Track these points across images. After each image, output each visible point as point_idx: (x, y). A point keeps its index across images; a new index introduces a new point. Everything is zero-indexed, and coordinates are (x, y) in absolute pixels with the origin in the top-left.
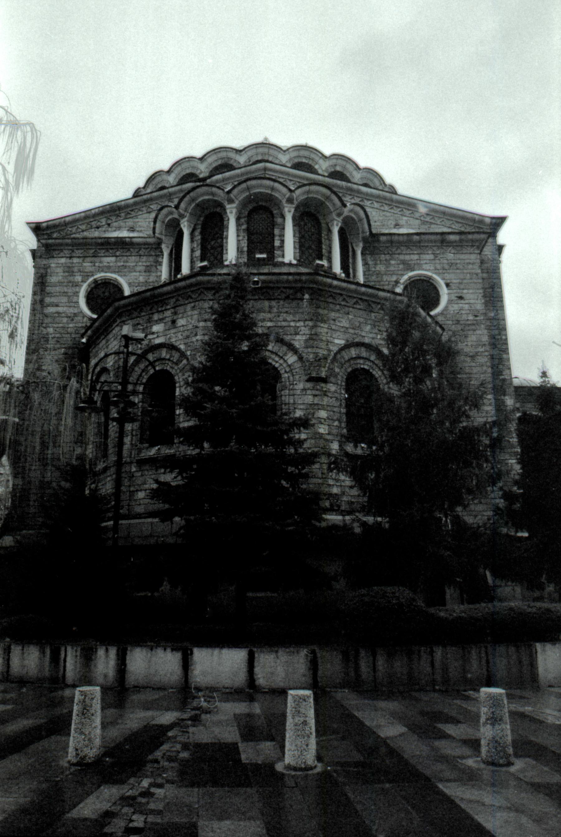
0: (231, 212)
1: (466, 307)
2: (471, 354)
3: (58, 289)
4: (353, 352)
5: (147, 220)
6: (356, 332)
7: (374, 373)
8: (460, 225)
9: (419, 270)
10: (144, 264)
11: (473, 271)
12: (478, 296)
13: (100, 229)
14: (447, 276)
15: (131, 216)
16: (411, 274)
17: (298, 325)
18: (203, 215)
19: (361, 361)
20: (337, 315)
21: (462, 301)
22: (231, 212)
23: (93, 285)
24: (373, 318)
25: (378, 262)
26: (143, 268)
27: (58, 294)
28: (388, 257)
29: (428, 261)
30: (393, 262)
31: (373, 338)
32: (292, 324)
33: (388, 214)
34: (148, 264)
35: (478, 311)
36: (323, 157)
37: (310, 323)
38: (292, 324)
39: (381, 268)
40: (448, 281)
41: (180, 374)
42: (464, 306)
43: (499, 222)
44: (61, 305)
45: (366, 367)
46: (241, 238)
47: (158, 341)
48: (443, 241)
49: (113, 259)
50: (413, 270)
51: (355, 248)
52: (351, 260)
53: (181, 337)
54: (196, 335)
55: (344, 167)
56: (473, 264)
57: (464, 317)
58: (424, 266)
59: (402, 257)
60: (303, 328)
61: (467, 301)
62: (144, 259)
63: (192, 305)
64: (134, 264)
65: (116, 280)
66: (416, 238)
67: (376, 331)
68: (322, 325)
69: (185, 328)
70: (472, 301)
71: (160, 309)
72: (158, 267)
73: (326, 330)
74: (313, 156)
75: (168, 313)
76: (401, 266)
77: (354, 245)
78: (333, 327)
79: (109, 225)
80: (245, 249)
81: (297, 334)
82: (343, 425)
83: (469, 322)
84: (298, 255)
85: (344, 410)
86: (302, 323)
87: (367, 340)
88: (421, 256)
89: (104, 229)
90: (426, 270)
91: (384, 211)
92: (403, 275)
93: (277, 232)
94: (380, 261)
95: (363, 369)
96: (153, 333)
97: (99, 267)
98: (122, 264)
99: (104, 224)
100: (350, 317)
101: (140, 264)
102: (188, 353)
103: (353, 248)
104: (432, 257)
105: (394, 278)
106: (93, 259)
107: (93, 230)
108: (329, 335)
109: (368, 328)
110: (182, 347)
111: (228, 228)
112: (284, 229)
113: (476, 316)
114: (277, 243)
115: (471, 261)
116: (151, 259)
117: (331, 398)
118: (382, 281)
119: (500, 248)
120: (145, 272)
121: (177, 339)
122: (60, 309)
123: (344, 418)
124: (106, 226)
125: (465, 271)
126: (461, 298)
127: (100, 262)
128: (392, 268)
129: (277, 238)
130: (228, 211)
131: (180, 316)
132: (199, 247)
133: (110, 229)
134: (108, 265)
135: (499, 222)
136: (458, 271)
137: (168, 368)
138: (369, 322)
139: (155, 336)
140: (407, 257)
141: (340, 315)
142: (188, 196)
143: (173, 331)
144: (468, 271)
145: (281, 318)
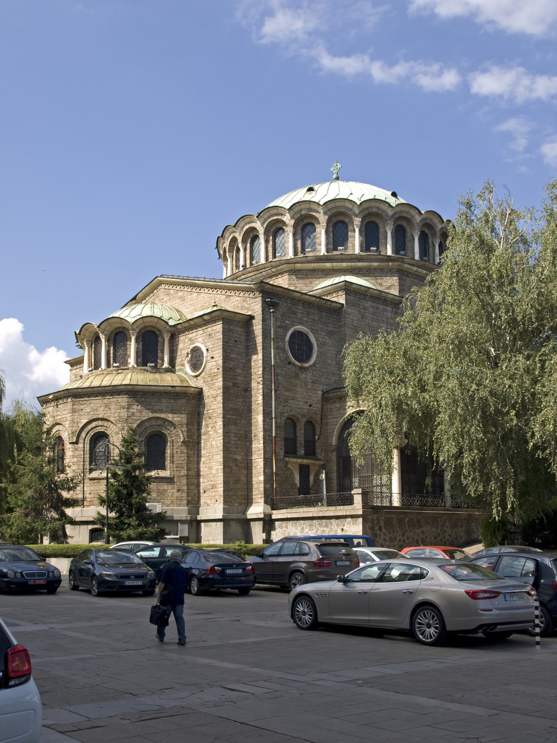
4: (94, 424)
6: (95, 412)
19: (100, 428)
20: (84, 406)
29: (200, 336)
30: (186, 340)
31: (105, 414)
32: (65, 416)
67: (107, 409)
73: (77, 416)
74: (280, 212)
78: (81, 414)
87: (100, 416)
95: (101, 431)
100: (91, 405)
108: (79, 418)
141: (86, 406)
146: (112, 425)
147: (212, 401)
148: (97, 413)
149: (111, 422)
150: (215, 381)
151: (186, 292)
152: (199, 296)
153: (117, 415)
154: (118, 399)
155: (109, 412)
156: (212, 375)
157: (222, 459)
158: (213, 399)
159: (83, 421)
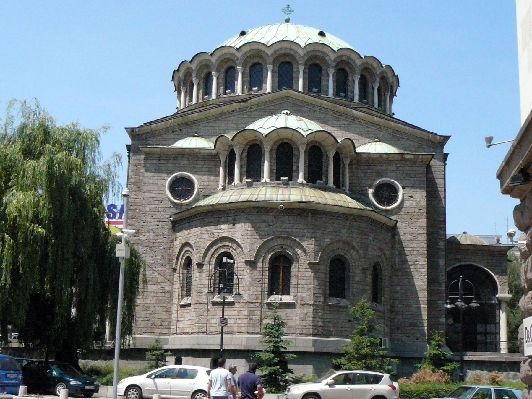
0: (267, 148)
1: (415, 203)
2: (415, 235)
3: (151, 181)
5: (207, 128)
7: (347, 257)
8: (419, 139)
9: (386, 177)
10: (208, 166)
11: (421, 179)
12: (423, 196)
13: (175, 133)
14: (404, 182)
15: (196, 124)
16: (379, 180)
17: (304, 231)
18: (249, 144)
21: (412, 199)
22: (267, 148)
23: (174, 179)
24: (348, 224)
25: (360, 171)
26: (207, 169)
27: (152, 185)
28: (366, 167)
30: (369, 171)
32: (302, 231)
33: (370, 130)
34: (210, 166)
35: (421, 206)
36: (333, 51)
37: (311, 231)
38: (302, 231)
39: (361, 175)
40: (405, 185)
41: (237, 256)
42: (413, 202)
43: (446, 138)
44: (153, 192)
45: (342, 254)
46: (272, 164)
47: (224, 235)
48: (403, 159)
49: (187, 162)
50: (382, 177)
51: (345, 162)
52: (341, 171)
53: (238, 235)
55: (349, 57)
56: (421, 174)
57: (412, 210)
58: (390, 174)
59: (375, 168)
60: (307, 233)
61: (415, 200)
62: (208, 162)
63: (245, 216)
64: (200, 166)
65: (189, 176)
66: (385, 156)
67: (350, 232)
68: (318, 232)
69: (241, 229)
70: (418, 199)
71: (226, 216)
72: (217, 169)
76: (374, 174)
77: (344, 160)
79: (181, 130)
80: (275, 171)
82: (327, 288)
83: (415, 214)
84: (307, 175)
85: (328, 280)
86: (306, 230)
87: (344, 238)
88: (389, 167)
89: (177, 133)
90: (390, 178)
91: (367, 127)
92: (375, 180)
93: (294, 160)
94: (361, 169)
96: (221, 229)
97: (178, 167)
98: (193, 166)
99: (177, 129)
101: (205, 166)
102: (242, 245)
103: (343, 162)
104: (395, 168)
105: (369, 182)
106: (175, 162)
107: (170, 133)
109: (344, 231)
110: (239, 241)
111: (264, 155)
112: (299, 158)
113: (421, 210)
114: (294, 168)
115: (420, 172)
116: (212, 163)
117: (321, 273)
118: (362, 183)
119: (446, 156)
121: (235, 235)
122: (153, 195)
123: (328, 284)
124: (179, 131)
125: (416, 179)
126: (411, 197)
127: (179, 164)
128: (368, 175)
129: (294, 164)
130: (265, 147)
132: (246, 166)
133: (181, 134)
134: (184, 166)
135: (446, 138)
136: (411, 179)
137: (230, 251)
138: (346, 227)
139: (223, 231)
140: (379, 168)
142: (240, 134)
143: (233, 230)
144: (418, 179)
145: (295, 227)
146: (352, 250)
147: (410, 240)
148: (340, 234)
149: (353, 247)
150: (415, 220)
151: (331, 117)
152: (351, 126)
153: (358, 240)
154: (360, 223)
155: (351, 235)
156: (410, 214)
157: (426, 299)
158: (412, 238)
159: (326, 240)
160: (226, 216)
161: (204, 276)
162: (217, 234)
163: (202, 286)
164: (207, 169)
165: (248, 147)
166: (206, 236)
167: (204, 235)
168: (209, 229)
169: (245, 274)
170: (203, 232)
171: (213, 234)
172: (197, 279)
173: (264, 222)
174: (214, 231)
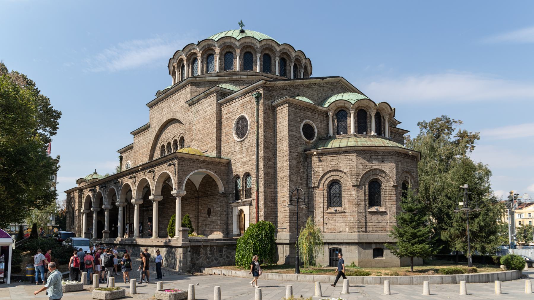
34: (321, 119)
54: (393, 169)
62: (320, 116)
63: (391, 157)
64: (317, 118)
71: (376, 155)
75: (380, 157)
81: (414, 172)
98: (313, 117)
101: (319, 118)
120: (320, 122)
131: (386, 160)
160: (376, 155)
161: (360, 193)
162: (371, 166)
163: (359, 200)
164: (319, 121)
165: (358, 110)
166: (361, 167)
167: (359, 166)
168: (363, 162)
169: (392, 193)
170: (359, 164)
171: (366, 166)
172: (353, 195)
173: (400, 161)
174: (368, 164)
